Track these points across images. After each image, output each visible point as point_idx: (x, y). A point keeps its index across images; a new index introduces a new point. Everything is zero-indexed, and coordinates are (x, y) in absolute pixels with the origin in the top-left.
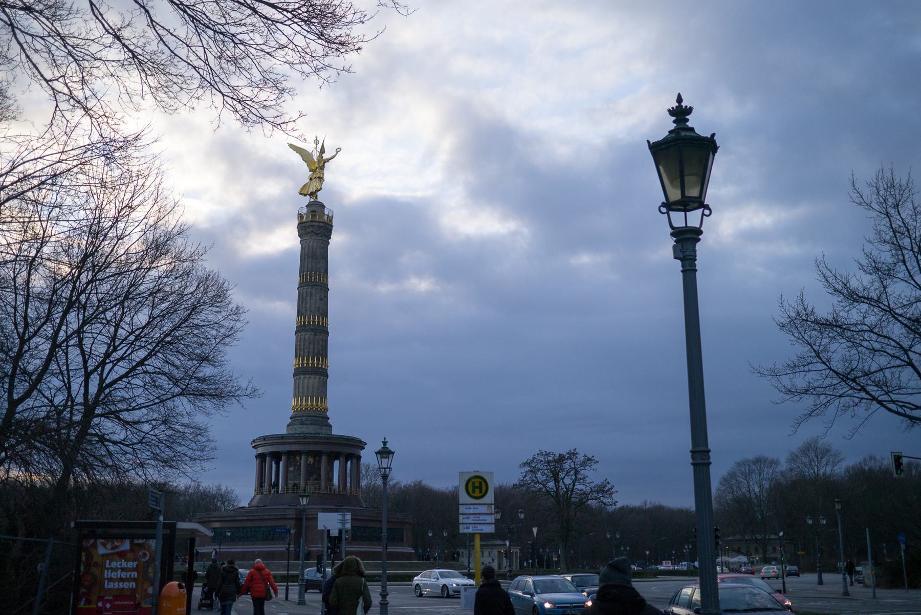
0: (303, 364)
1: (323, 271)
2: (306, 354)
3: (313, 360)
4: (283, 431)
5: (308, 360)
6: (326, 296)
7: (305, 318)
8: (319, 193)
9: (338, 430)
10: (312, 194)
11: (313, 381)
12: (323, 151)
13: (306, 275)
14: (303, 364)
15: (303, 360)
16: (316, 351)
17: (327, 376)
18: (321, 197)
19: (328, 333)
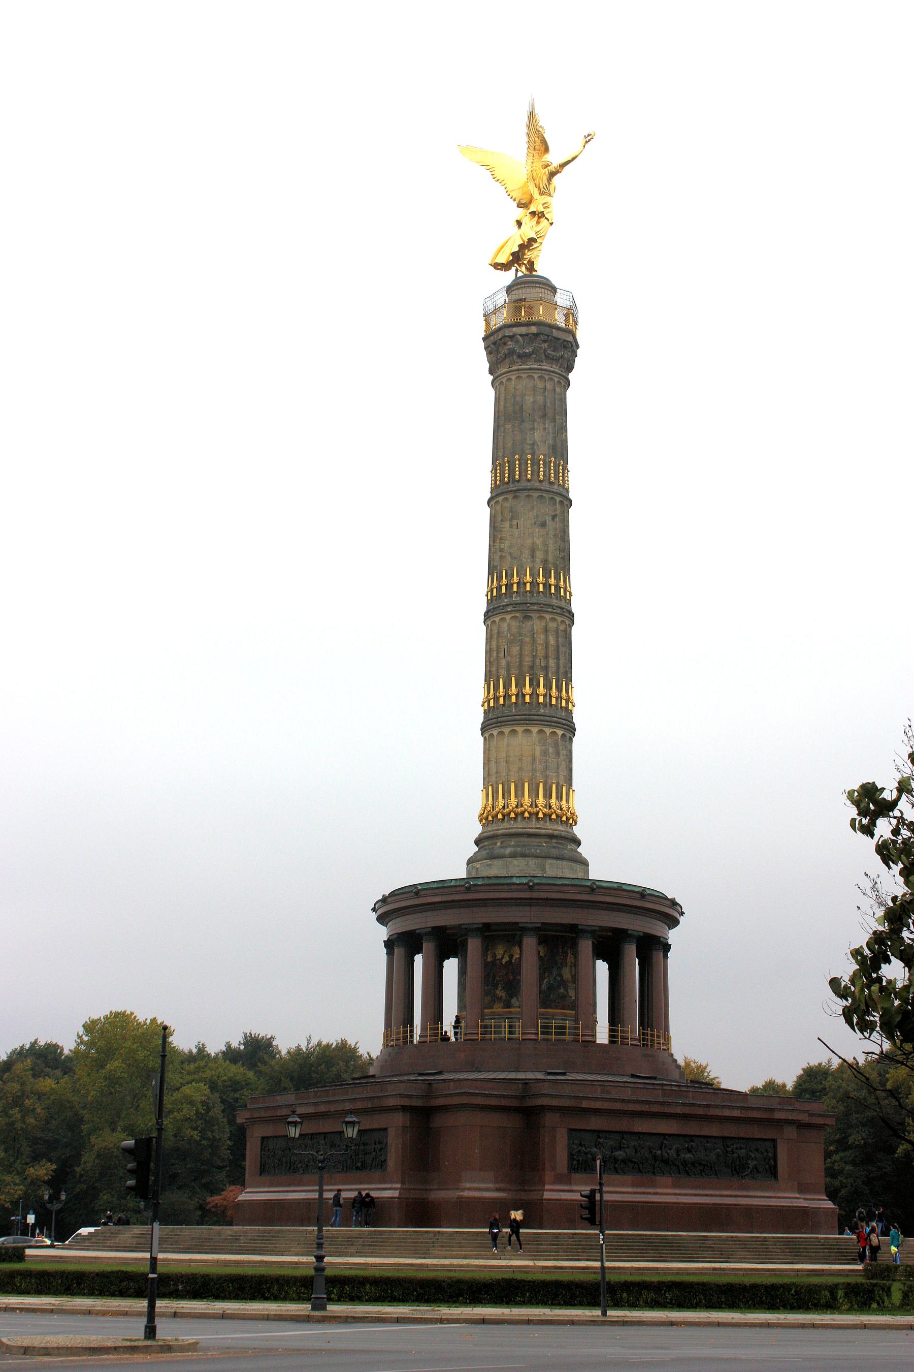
0: (507, 696)
4: (459, 872)
9: (602, 869)
14: (507, 696)
15: (507, 686)
19: (571, 616)
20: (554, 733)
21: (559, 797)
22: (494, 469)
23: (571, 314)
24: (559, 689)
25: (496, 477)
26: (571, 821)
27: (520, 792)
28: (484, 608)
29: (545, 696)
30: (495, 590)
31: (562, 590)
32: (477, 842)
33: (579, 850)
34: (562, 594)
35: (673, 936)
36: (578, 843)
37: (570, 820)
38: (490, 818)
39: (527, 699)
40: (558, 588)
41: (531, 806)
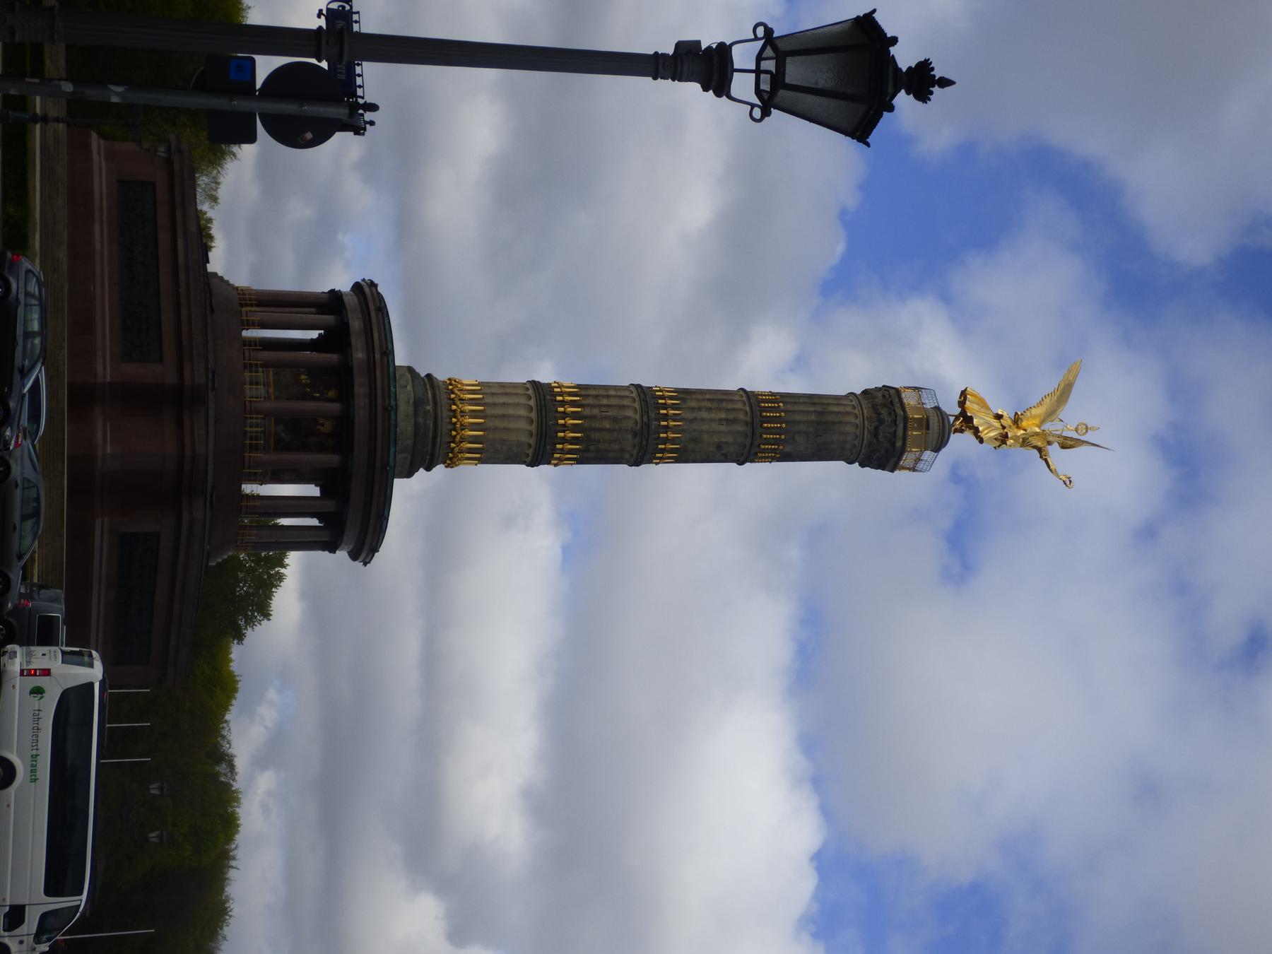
1: (788, 449)
2: (587, 412)
3: (575, 428)
5: (574, 416)
6: (725, 458)
7: (674, 407)
8: (968, 435)
11: (522, 428)
12: (1067, 444)
13: (777, 409)
14: (563, 403)
15: (573, 404)
16: (596, 436)
17: (533, 464)
18: (960, 442)
19: (637, 463)
21: (471, 451)
22: (772, 394)
24: (571, 451)
28: (644, 384)
29: (563, 438)
32: (429, 376)
35: (342, 555)
36: (428, 469)
37: (451, 463)
40: (662, 451)
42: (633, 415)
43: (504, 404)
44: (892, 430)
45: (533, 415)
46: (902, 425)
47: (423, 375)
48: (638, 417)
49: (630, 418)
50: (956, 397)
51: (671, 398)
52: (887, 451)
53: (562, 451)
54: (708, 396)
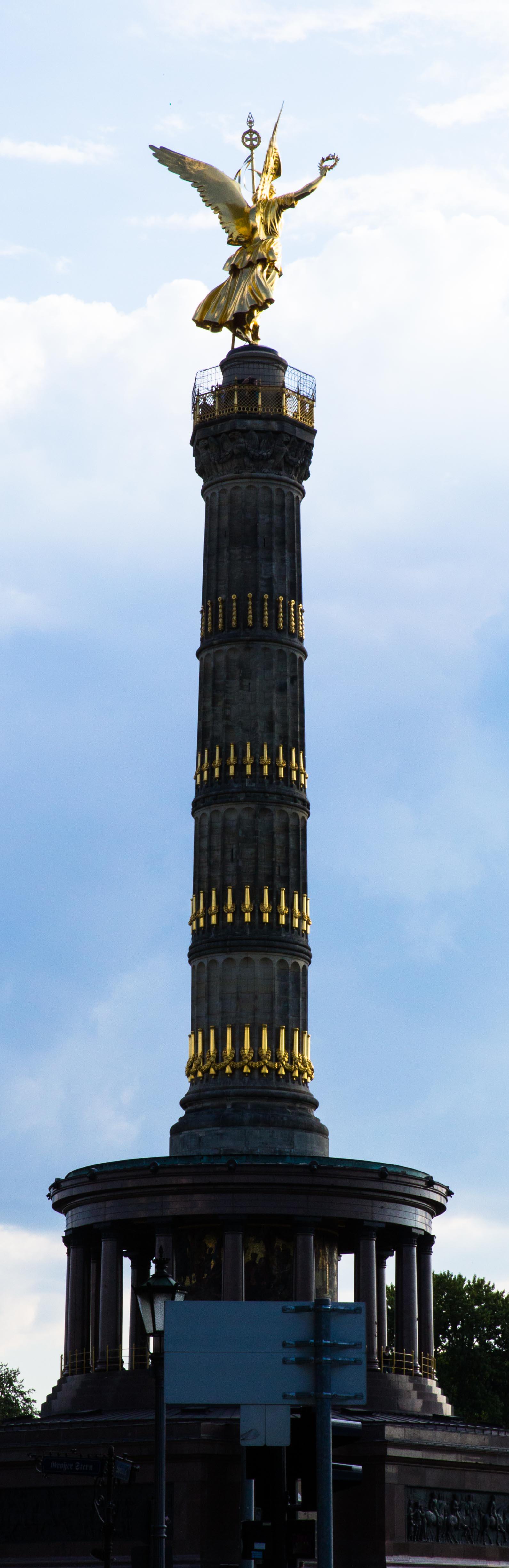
6: (298, 678)
7: (225, 755)
8: (260, 318)
10: (240, 323)
13: (227, 603)
14: (221, 915)
17: (308, 957)
19: (306, 805)
20: (282, 962)
21: (289, 1047)
22: (204, 611)
23: (307, 402)
25: (207, 622)
26: (305, 1076)
27: (237, 1043)
30: (205, 773)
31: (294, 773)
32: (184, 1104)
33: (317, 1114)
34: (295, 778)
38: (200, 1074)
39: (247, 917)
41: (253, 1059)
42: (237, 813)
43: (222, 999)
44: (256, 436)
45: (238, 957)
46: (249, 422)
47: (182, 1113)
48: (239, 808)
49: (240, 819)
50: (206, 333)
51: (212, 758)
52: (286, 443)
53: (290, 916)
54: (209, 704)
